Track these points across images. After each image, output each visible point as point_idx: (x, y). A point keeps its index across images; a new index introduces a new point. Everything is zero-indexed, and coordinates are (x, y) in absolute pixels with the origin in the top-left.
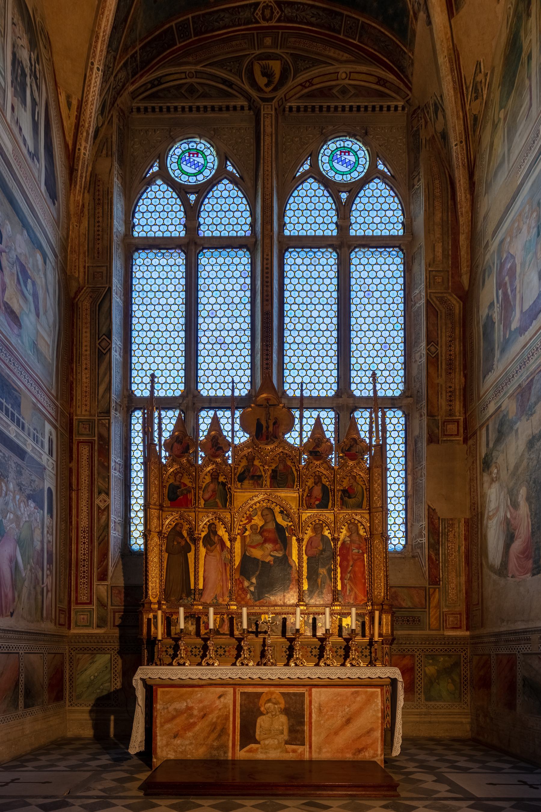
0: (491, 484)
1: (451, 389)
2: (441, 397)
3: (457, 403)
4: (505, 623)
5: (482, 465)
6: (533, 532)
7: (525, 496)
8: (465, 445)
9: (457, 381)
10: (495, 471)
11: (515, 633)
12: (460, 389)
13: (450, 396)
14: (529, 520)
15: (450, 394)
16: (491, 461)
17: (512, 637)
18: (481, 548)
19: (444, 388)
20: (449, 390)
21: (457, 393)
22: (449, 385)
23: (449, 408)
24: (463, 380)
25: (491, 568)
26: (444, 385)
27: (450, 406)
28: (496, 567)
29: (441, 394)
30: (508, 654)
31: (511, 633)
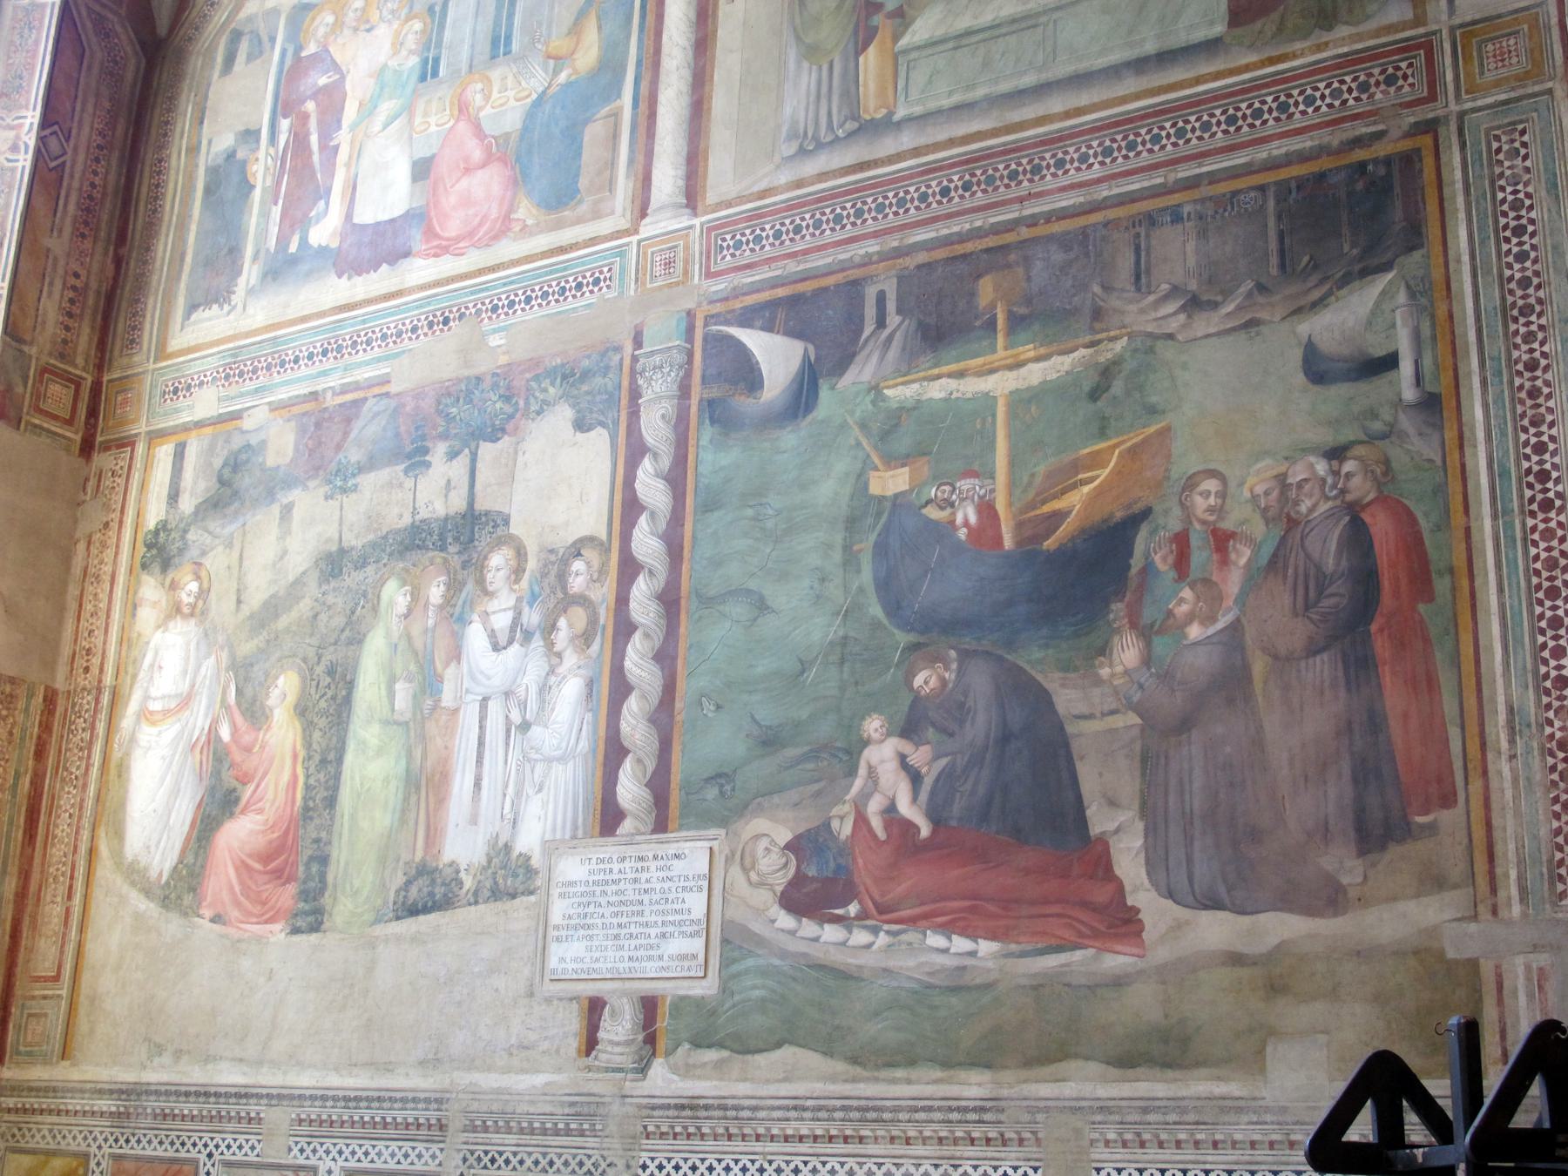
0: (169, 617)
1: (78, 283)
2: (50, 294)
3: (86, 330)
4: (166, 1059)
5: (141, 549)
6: (306, 809)
7: (291, 699)
8: (81, 461)
9: (95, 267)
10: (193, 586)
11: (204, 1094)
12: (98, 293)
13: (72, 301)
14: (300, 771)
15: (71, 294)
16: (181, 551)
17: (187, 1107)
18: (98, 799)
19: (61, 271)
20: (72, 281)
21: (91, 302)
22: (75, 266)
23: (63, 334)
24: (110, 268)
25: (134, 874)
26: (62, 262)
27: (67, 328)
28: (153, 874)
29: (51, 284)
30: (161, 1160)
31: (187, 1094)
